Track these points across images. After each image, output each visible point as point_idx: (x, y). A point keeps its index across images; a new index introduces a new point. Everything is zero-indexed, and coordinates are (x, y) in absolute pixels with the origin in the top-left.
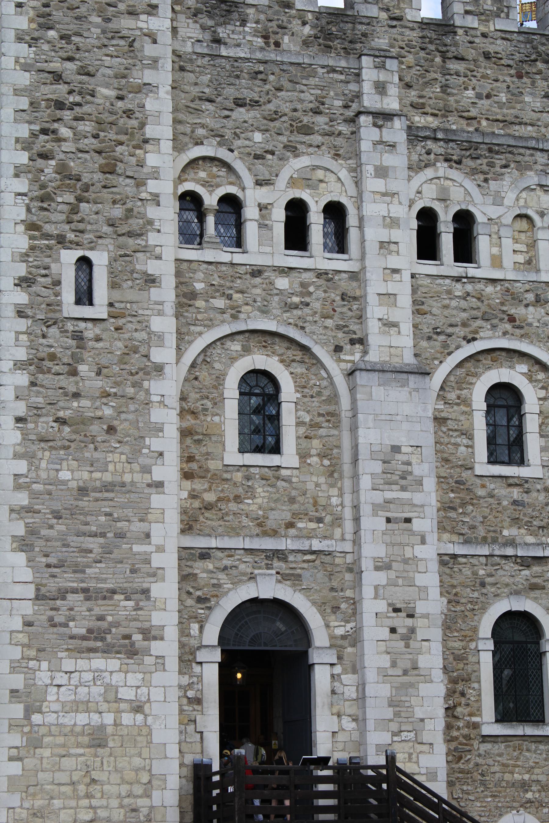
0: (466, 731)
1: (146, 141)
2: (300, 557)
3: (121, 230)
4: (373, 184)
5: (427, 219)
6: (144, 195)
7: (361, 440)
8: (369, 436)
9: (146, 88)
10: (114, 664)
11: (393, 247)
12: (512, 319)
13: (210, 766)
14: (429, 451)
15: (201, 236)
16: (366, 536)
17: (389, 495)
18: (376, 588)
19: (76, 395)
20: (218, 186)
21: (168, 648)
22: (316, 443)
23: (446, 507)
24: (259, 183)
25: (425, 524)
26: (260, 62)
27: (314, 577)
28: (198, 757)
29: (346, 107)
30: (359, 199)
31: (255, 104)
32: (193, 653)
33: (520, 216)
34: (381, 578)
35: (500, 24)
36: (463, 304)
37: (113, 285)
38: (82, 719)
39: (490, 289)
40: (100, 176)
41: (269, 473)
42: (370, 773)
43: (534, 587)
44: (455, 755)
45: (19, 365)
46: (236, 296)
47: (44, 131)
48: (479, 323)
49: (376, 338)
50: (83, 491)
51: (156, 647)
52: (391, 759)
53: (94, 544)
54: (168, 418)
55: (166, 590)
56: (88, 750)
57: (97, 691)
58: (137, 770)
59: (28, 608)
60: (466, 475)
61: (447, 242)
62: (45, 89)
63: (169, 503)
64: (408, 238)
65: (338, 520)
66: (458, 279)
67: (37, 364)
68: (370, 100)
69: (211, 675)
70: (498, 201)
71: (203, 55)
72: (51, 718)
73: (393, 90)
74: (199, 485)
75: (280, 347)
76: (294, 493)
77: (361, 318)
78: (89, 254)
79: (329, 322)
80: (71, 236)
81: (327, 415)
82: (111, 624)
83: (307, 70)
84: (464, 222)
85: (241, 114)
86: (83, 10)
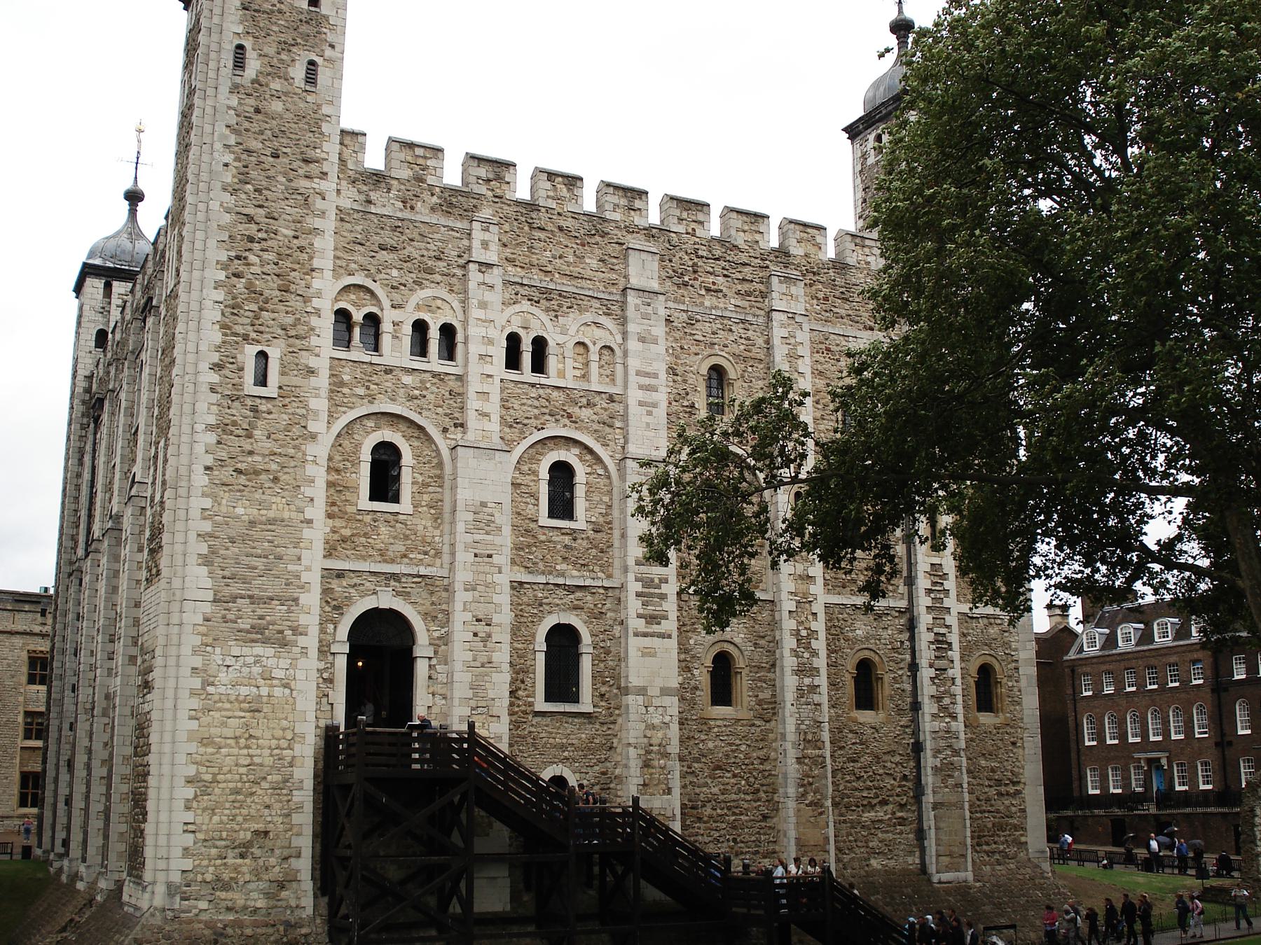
0: (523, 708)
1: (313, 270)
2: (410, 579)
3: (292, 333)
4: (476, 313)
5: (513, 341)
6: (309, 310)
7: (458, 497)
8: (465, 494)
9: (316, 231)
10: (270, 651)
11: (488, 359)
12: (570, 416)
13: (338, 728)
14: (507, 506)
15: (349, 342)
16: (459, 565)
17: (478, 537)
18: (465, 603)
19: (251, 453)
20: (364, 306)
21: (311, 641)
22: (426, 497)
23: (518, 548)
24: (393, 306)
25: (502, 559)
26: (399, 219)
27: (419, 594)
28: (329, 722)
29: (459, 256)
30: (465, 323)
31: (394, 249)
32: (329, 646)
33: (578, 343)
34: (469, 596)
36: (536, 403)
37: (283, 374)
38: (244, 691)
39: (555, 394)
40: (278, 293)
41: (391, 517)
42: (455, 735)
43: (576, 608)
44: (515, 725)
45: (210, 428)
46: (372, 387)
47: (238, 258)
48: (547, 417)
49: (472, 421)
50: (252, 523)
51: (302, 641)
52: (471, 726)
53: (259, 563)
54: (319, 474)
55: (312, 599)
56: (248, 714)
57: (256, 670)
58: (284, 730)
59: (208, 608)
60: (532, 525)
61: (527, 359)
62: (241, 227)
63: (317, 535)
64: (499, 352)
65: (438, 554)
66: (533, 385)
67: (223, 428)
68: (478, 254)
69: (341, 663)
71: (358, 211)
72: (222, 690)
73: (495, 247)
74: (338, 523)
75: (403, 427)
76: (408, 532)
77: (462, 408)
78: (266, 349)
79: (439, 410)
80: (253, 335)
82: (269, 623)
84: (540, 345)
86: (271, 173)
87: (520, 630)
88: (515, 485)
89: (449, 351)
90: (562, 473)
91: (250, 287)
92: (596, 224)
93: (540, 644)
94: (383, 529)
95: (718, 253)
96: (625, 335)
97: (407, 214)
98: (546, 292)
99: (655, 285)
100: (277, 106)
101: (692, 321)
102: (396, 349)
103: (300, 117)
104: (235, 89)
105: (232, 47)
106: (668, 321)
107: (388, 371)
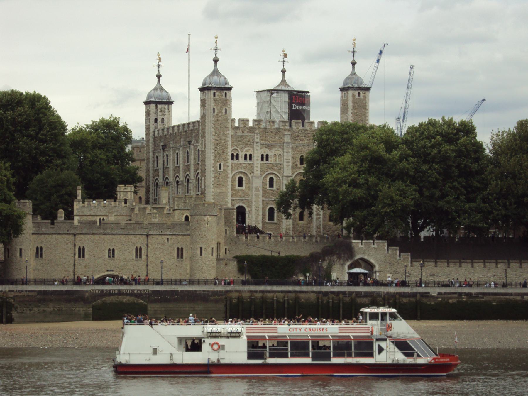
4: (256, 152)
5: (262, 156)
8: (254, 185)
9: (228, 141)
23: (263, 194)
25: (260, 196)
30: (254, 153)
35: (273, 127)
44: (263, 225)
54: (230, 183)
61: (265, 159)
63: (229, 194)
64: (260, 158)
67: (215, 177)
68: (256, 140)
70: (272, 152)
77: (253, 169)
81: (249, 182)
83: (248, 136)
84: (267, 156)
85: (240, 143)
87: (264, 209)
88: (263, 182)
89: (250, 159)
90: (271, 180)
91: (218, 153)
92: (278, 130)
93: (267, 211)
94: (240, 192)
95: (303, 131)
96: (283, 152)
97: (243, 134)
98: (269, 145)
99: (290, 141)
100: (220, 119)
101: (297, 147)
102: (241, 160)
103: (224, 120)
104: (213, 116)
105: (212, 109)
106: (292, 148)
107: (240, 164)
